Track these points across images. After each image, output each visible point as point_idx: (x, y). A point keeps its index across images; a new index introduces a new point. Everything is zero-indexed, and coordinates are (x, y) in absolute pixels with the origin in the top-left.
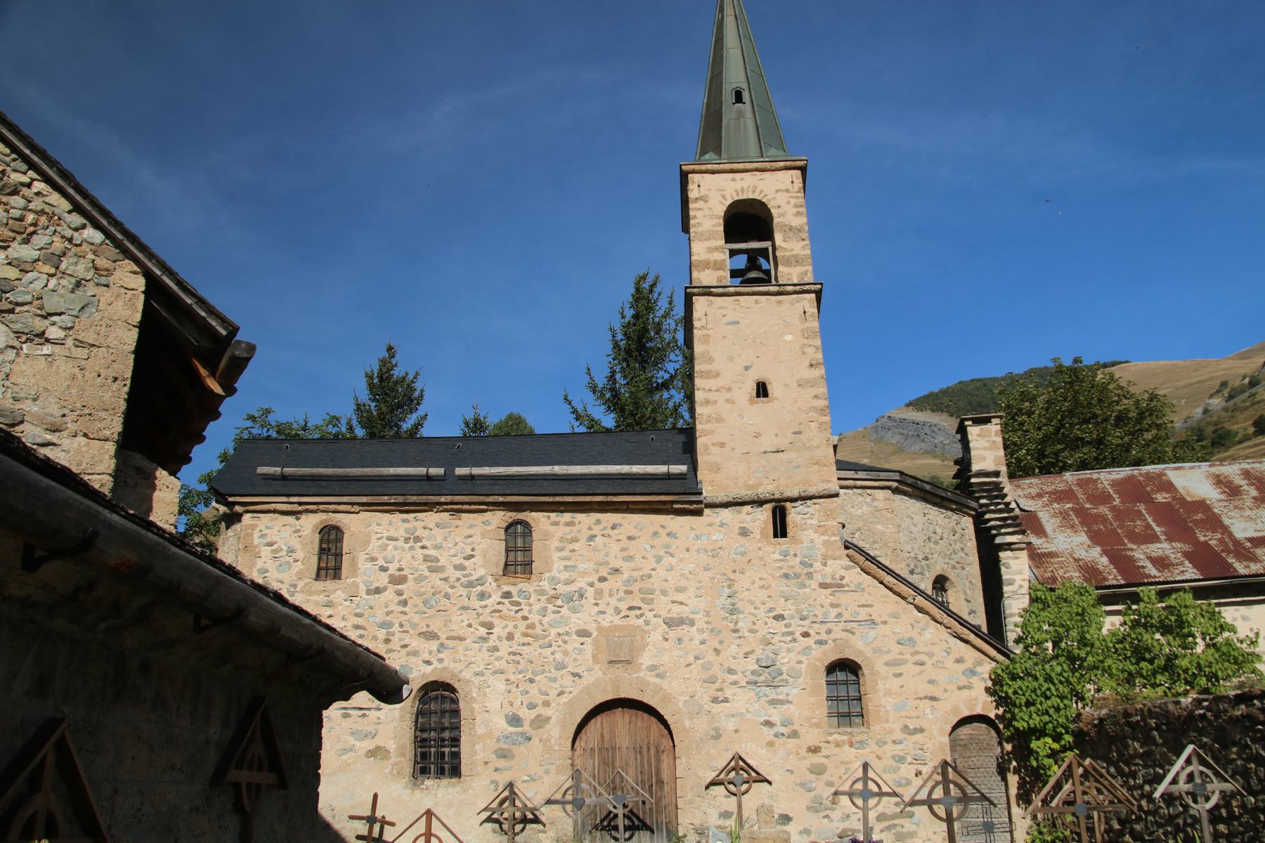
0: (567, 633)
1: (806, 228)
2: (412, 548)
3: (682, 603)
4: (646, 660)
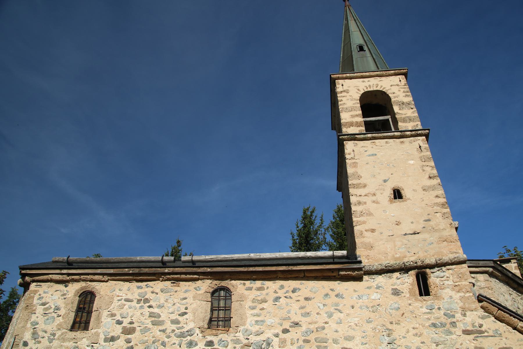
2: (142, 307)
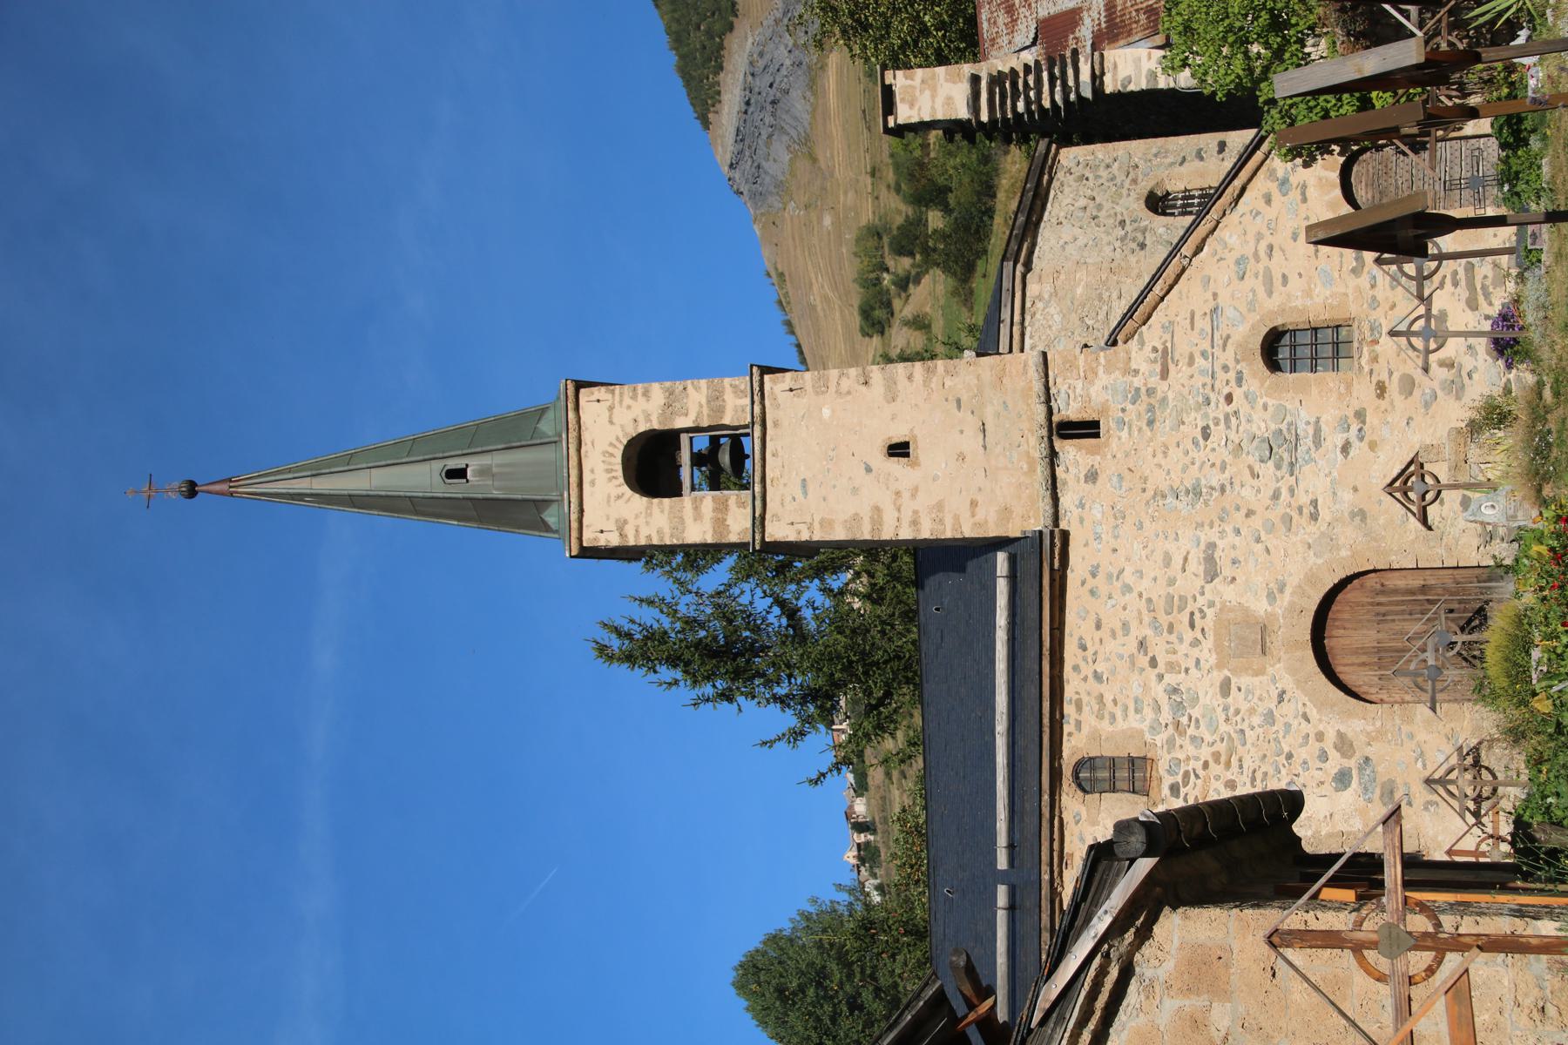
0: (1226, 709)
1: (668, 384)
3: (1186, 559)
4: (1260, 607)
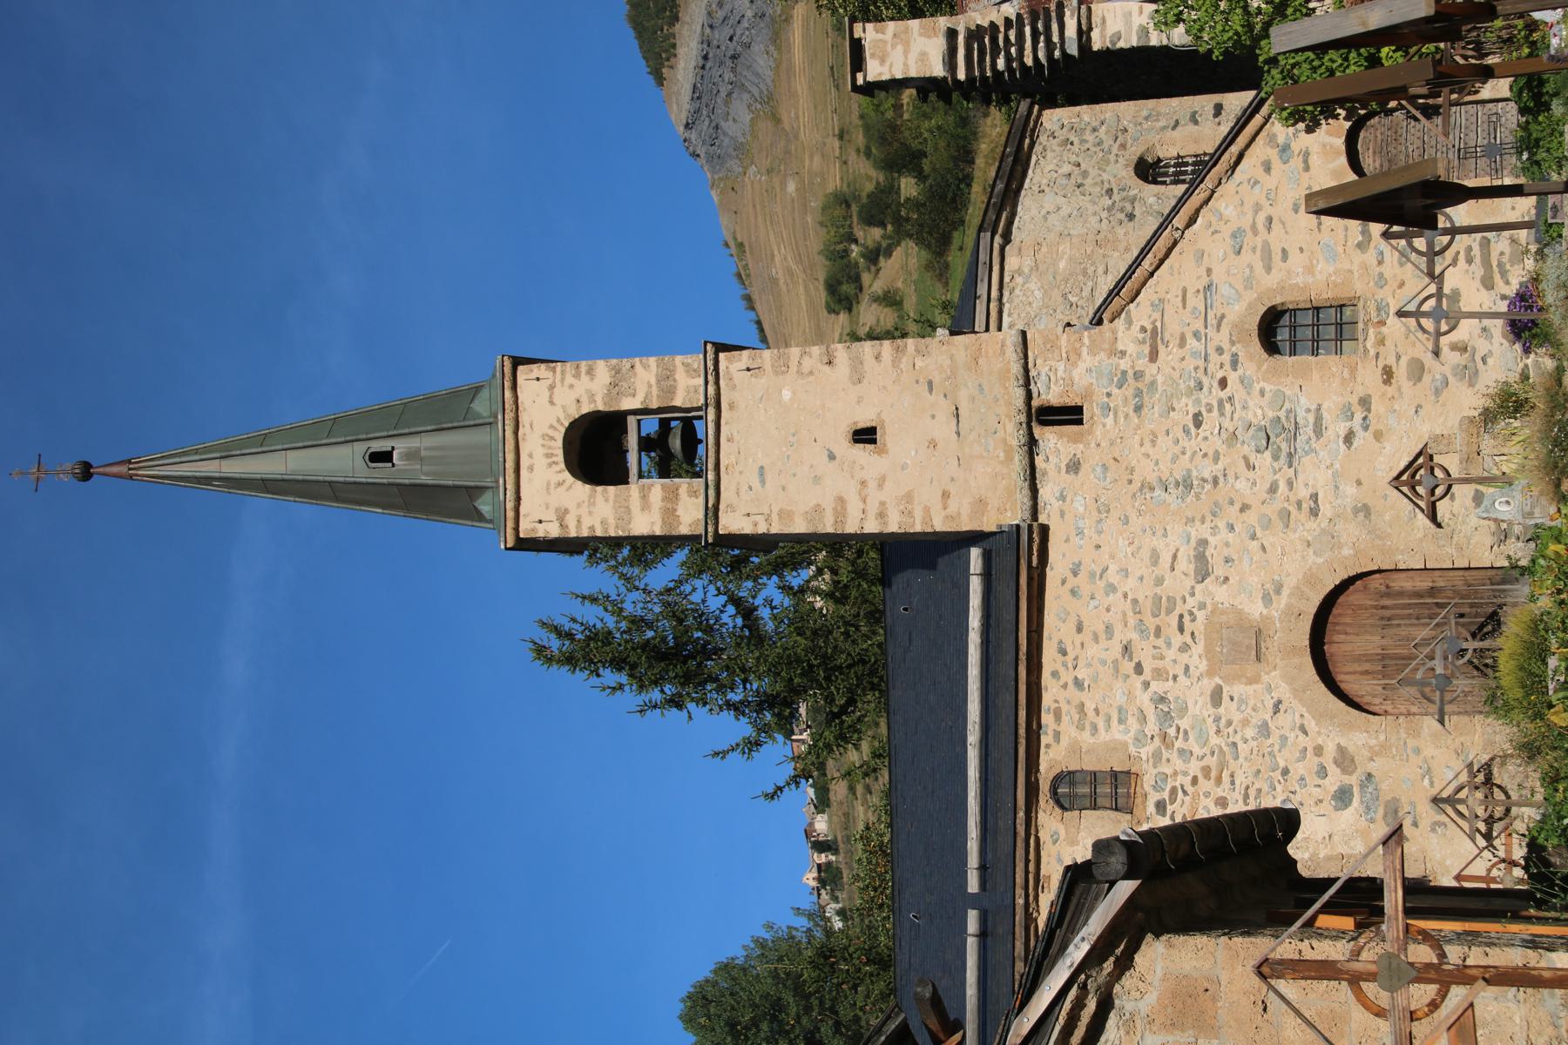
0: (1217, 719)
1: (614, 361)
3: (1175, 557)
4: (1255, 609)
